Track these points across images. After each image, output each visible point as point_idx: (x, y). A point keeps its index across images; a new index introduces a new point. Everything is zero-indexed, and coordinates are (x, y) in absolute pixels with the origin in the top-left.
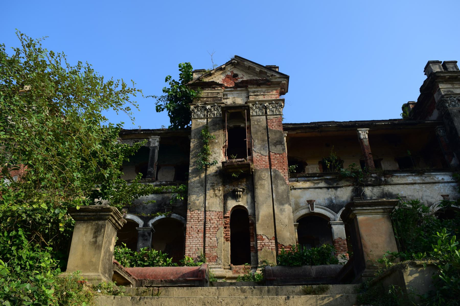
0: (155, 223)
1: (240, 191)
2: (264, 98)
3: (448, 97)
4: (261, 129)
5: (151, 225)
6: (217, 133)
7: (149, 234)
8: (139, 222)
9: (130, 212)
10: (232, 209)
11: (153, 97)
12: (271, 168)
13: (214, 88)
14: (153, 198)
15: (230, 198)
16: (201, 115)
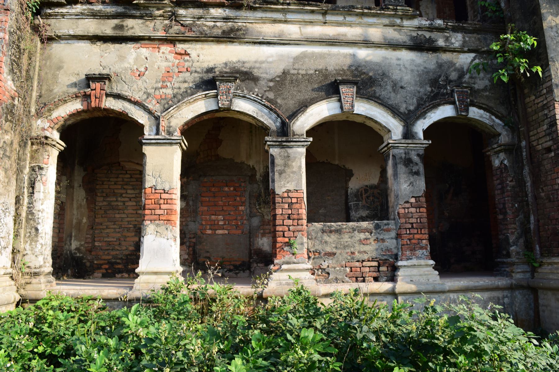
8: (391, 124)
14: (413, 60)
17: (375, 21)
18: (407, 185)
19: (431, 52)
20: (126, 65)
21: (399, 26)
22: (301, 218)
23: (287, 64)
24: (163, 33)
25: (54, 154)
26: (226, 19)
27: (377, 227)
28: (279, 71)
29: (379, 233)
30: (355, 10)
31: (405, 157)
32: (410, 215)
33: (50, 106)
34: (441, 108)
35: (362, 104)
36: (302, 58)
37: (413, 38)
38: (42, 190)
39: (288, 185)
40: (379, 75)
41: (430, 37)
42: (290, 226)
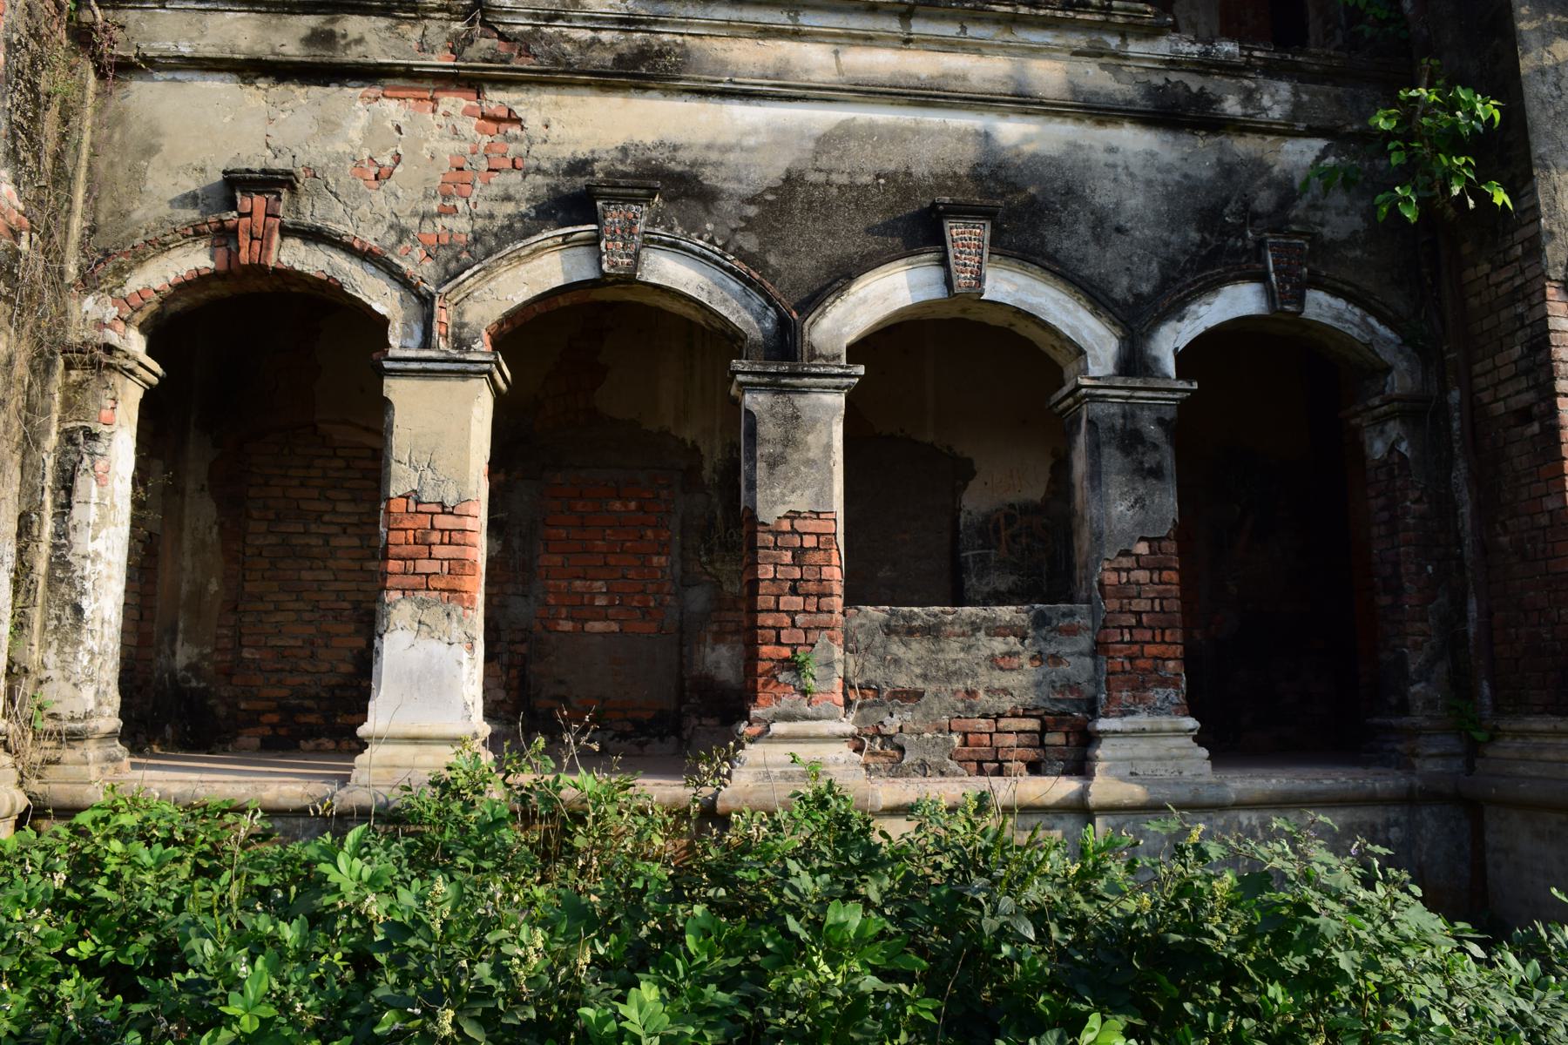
8: (1085, 333)
14: (1153, 155)
17: (1049, 40)
18: (1126, 504)
19: (1203, 133)
20: (341, 147)
21: (1115, 55)
22: (827, 591)
23: (798, 154)
24: (448, 58)
25: (132, 394)
27: (1040, 621)
28: (776, 175)
29: (1045, 639)
30: (994, 7)
31: (1124, 425)
32: (1134, 590)
33: (122, 259)
34: (1228, 290)
35: (1006, 274)
36: (841, 138)
37: (1152, 91)
38: (94, 499)
39: (793, 498)
40: (1055, 192)
41: (1202, 89)
42: (796, 612)
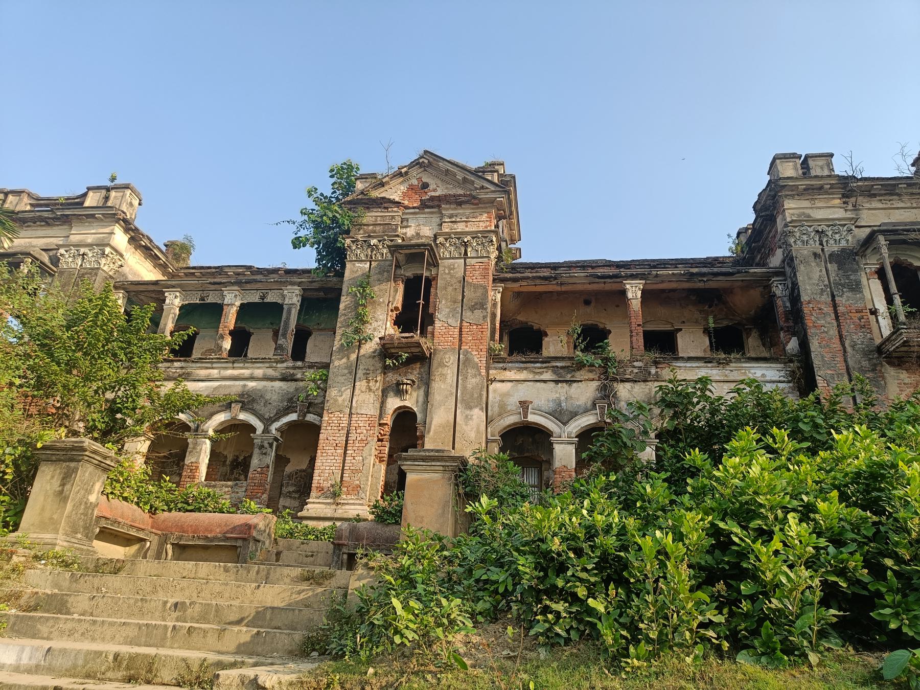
0: (281, 427)
1: (407, 384)
2: (467, 226)
3: (796, 227)
4: (454, 281)
5: (274, 432)
6: (384, 286)
7: (271, 445)
9: (244, 408)
10: (394, 412)
11: (288, 222)
12: (460, 349)
13: (387, 208)
15: (392, 394)
16: (362, 255)
26: (182, 368)
34: (290, 415)
